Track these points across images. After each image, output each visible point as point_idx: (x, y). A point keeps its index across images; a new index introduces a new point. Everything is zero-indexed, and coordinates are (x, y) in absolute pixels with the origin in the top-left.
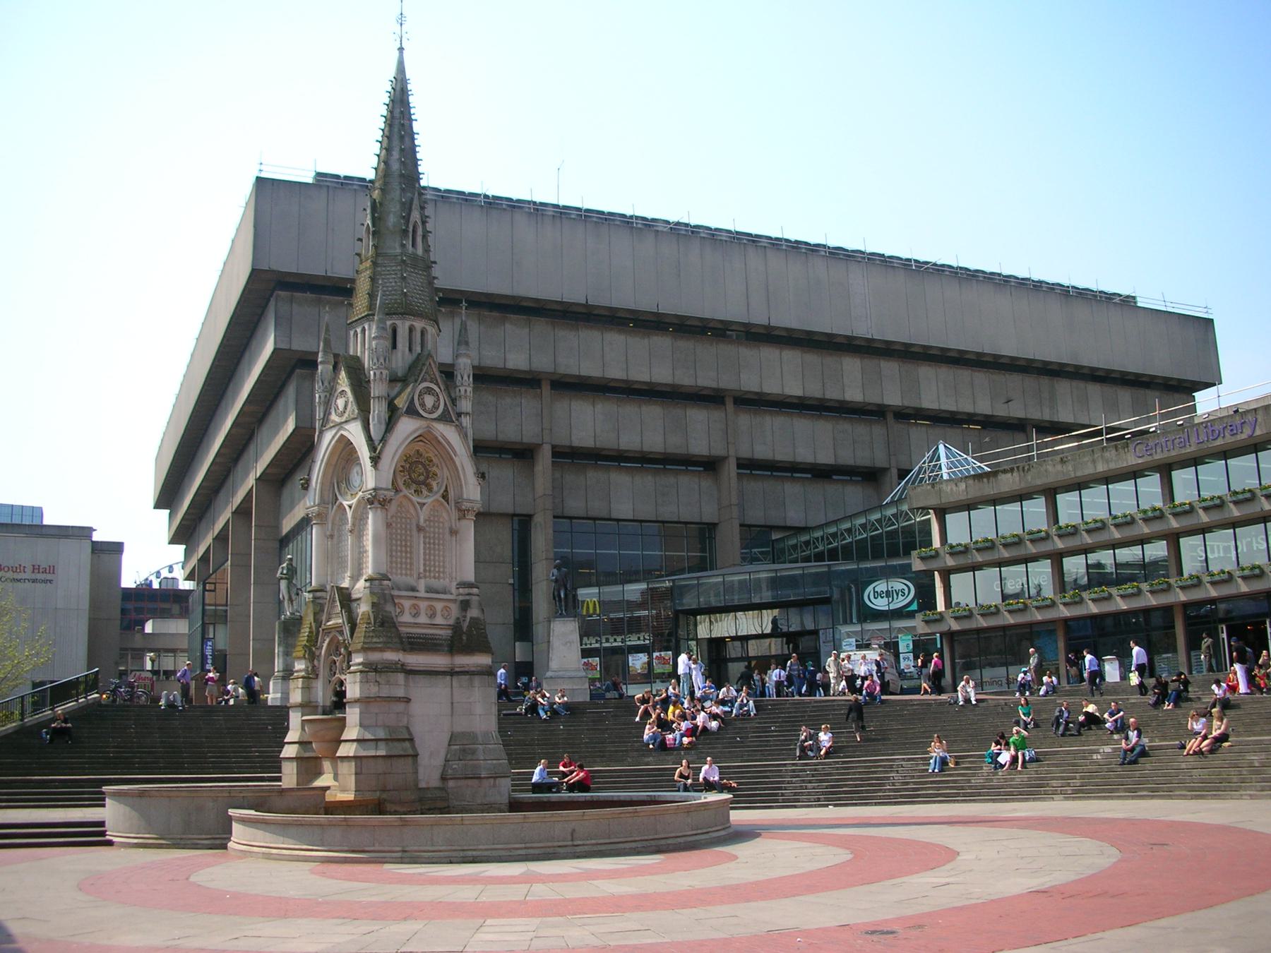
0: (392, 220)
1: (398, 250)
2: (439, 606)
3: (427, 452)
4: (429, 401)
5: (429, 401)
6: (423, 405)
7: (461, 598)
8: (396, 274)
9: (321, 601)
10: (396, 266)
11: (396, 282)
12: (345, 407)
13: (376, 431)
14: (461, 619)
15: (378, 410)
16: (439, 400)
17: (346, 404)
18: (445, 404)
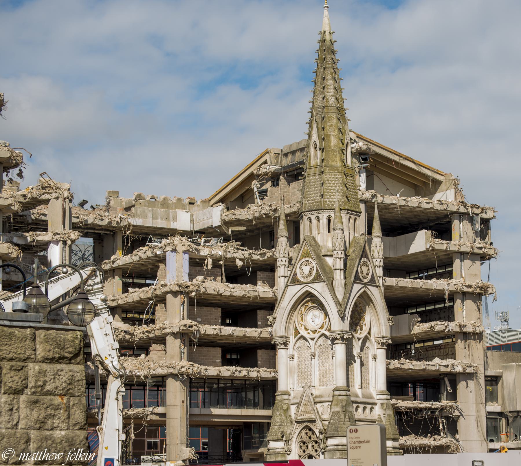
0: (334, 141)
1: (339, 163)
2: (369, 407)
3: (360, 304)
4: (365, 269)
5: (365, 269)
6: (362, 272)
7: (382, 401)
8: (339, 181)
9: (287, 402)
10: (338, 175)
11: (339, 186)
12: (310, 273)
13: (340, 293)
14: (382, 416)
15: (339, 277)
16: (369, 269)
17: (311, 270)
18: (372, 272)
